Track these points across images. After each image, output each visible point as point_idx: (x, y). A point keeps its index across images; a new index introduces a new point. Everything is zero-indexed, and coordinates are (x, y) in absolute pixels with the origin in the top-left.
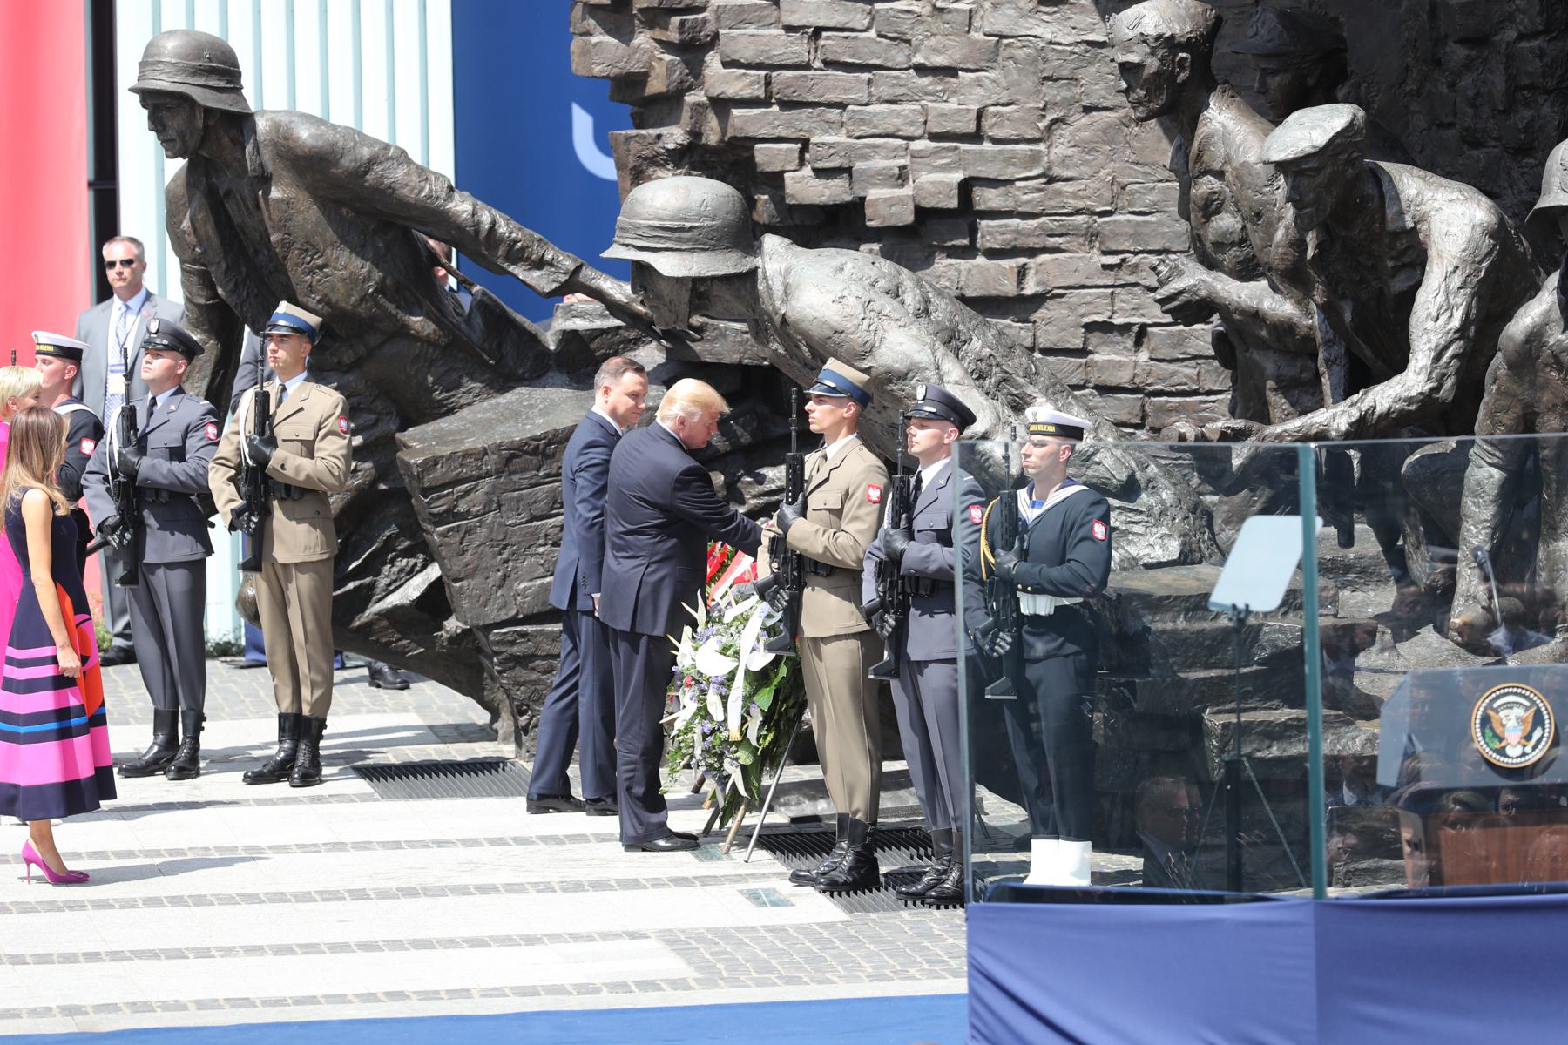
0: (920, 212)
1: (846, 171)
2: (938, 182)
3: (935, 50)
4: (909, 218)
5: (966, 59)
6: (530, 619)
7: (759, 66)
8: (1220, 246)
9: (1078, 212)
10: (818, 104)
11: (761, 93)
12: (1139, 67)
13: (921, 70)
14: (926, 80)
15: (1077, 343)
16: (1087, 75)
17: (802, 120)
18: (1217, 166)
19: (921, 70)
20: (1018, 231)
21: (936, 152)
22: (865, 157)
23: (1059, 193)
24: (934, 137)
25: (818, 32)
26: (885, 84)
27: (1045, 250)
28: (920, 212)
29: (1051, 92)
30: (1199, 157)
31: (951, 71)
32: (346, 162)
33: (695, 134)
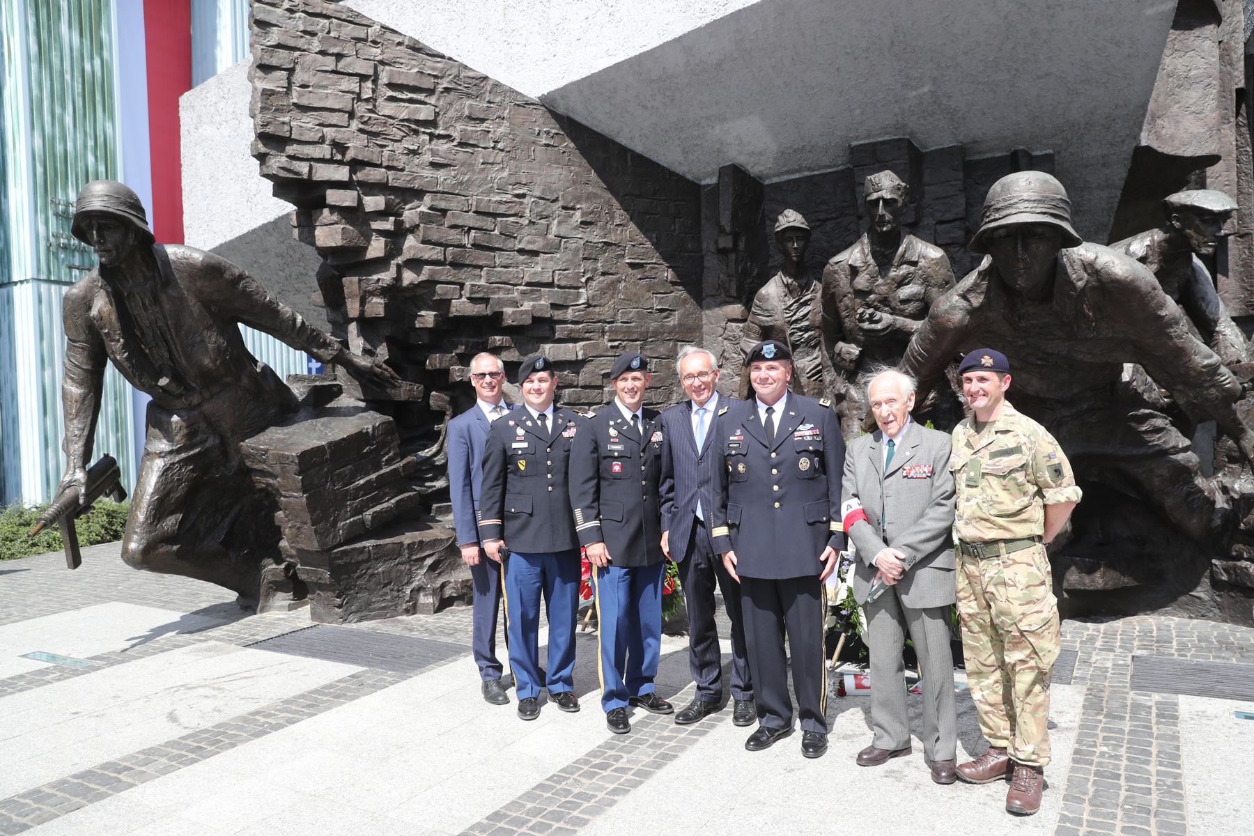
0: (534, 318)
1: (486, 300)
2: (541, 303)
3: (529, 242)
4: (529, 322)
5: (544, 247)
6: (347, 542)
7: (440, 245)
8: (904, 302)
9: (599, 321)
10: (468, 266)
11: (442, 258)
12: (893, 200)
13: (521, 251)
14: (522, 258)
15: (599, 383)
16: (602, 259)
17: (462, 275)
18: (915, 259)
19: (521, 251)
20: (572, 331)
21: (532, 291)
22: (494, 293)
23: (592, 313)
24: (528, 284)
25: (470, 229)
26: (499, 258)
27: (583, 340)
28: (534, 318)
29: (589, 265)
30: (903, 255)
31: (535, 253)
32: (227, 275)
33: (399, 278)
